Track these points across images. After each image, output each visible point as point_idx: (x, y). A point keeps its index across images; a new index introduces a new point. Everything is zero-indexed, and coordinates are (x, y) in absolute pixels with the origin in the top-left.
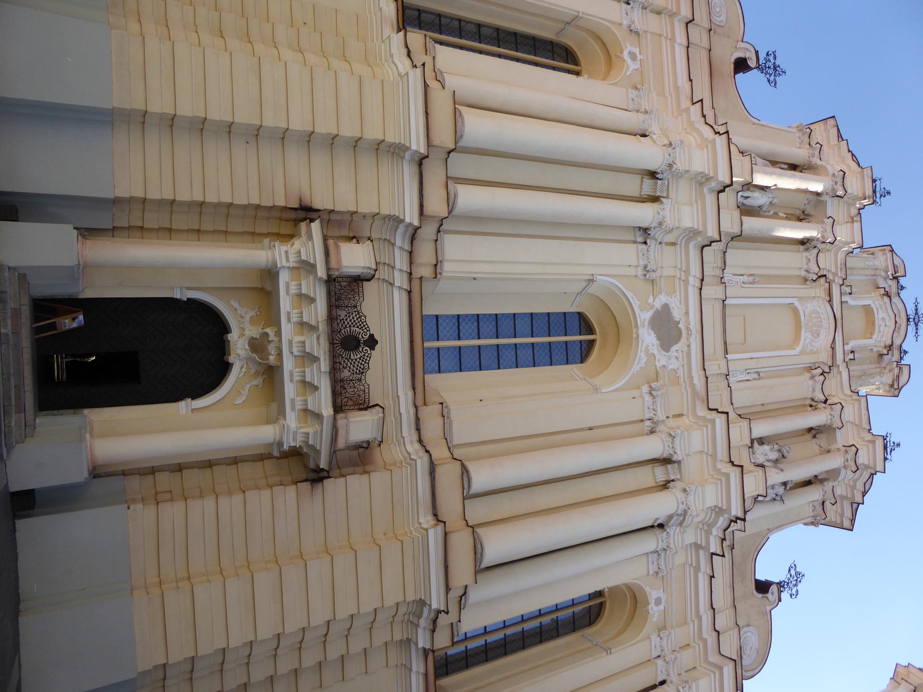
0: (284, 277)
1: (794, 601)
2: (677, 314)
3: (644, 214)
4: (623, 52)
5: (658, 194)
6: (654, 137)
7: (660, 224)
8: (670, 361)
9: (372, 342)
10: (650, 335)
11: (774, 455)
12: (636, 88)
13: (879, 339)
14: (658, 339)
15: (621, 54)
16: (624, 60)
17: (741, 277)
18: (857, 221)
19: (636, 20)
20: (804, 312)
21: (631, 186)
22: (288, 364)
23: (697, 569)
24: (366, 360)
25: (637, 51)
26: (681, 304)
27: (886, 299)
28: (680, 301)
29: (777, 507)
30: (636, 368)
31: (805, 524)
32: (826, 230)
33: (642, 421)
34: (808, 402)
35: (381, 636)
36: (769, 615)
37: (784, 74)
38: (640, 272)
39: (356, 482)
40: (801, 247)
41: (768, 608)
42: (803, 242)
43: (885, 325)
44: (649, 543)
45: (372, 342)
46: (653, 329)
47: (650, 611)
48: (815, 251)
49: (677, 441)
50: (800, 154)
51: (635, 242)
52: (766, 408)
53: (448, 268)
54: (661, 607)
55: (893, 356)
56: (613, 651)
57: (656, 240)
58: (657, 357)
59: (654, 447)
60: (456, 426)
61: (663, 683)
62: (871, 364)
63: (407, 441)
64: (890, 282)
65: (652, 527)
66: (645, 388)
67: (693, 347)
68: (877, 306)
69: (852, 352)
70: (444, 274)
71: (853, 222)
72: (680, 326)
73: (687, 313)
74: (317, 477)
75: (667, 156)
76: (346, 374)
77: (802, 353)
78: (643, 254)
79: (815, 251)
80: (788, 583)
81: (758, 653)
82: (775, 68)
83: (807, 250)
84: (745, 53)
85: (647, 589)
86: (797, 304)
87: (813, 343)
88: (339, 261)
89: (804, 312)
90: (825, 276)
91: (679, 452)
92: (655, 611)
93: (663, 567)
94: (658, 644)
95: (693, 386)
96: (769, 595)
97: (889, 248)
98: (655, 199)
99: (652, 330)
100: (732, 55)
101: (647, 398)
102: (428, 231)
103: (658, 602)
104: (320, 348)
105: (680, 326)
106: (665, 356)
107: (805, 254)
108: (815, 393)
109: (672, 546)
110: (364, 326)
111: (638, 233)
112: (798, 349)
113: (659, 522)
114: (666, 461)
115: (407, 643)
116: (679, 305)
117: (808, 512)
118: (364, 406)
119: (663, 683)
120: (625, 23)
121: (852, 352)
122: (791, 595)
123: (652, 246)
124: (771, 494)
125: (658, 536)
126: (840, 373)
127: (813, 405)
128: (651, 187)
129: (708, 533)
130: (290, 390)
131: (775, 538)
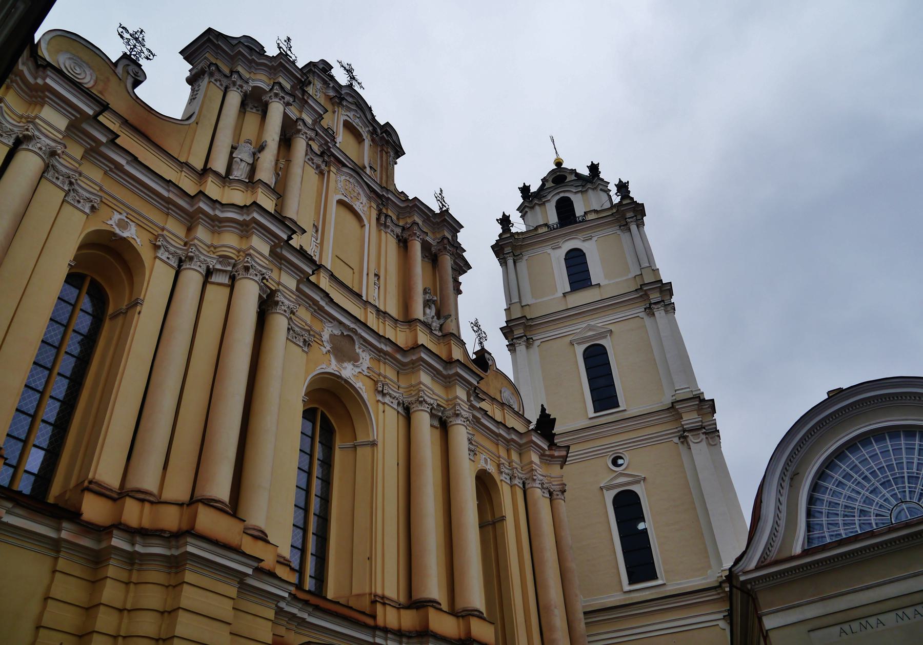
2: (337, 332)
4: (114, 234)
6: (218, 267)
10: (345, 368)
12: (158, 247)
13: (366, 134)
14: (350, 361)
15: (116, 237)
16: (124, 238)
18: (308, 98)
19: (88, 195)
20: (343, 194)
25: (117, 216)
26: (331, 322)
28: (330, 322)
32: (306, 133)
36: (498, 371)
37: (143, 33)
41: (495, 369)
43: (358, 118)
47: (490, 471)
56: (504, 515)
58: (361, 371)
66: (380, 398)
67: (364, 334)
68: (345, 114)
71: (307, 102)
72: (345, 334)
73: (340, 323)
75: (256, 278)
77: (370, 223)
78: (296, 338)
84: (128, 73)
89: (343, 194)
92: (491, 468)
95: (386, 353)
97: (311, 65)
99: (343, 363)
100: (129, 93)
101: (387, 400)
105: (345, 334)
106: (361, 363)
108: (395, 232)
112: (366, 222)
116: (331, 325)
120: (87, 211)
126: (388, 199)
128: (224, 276)
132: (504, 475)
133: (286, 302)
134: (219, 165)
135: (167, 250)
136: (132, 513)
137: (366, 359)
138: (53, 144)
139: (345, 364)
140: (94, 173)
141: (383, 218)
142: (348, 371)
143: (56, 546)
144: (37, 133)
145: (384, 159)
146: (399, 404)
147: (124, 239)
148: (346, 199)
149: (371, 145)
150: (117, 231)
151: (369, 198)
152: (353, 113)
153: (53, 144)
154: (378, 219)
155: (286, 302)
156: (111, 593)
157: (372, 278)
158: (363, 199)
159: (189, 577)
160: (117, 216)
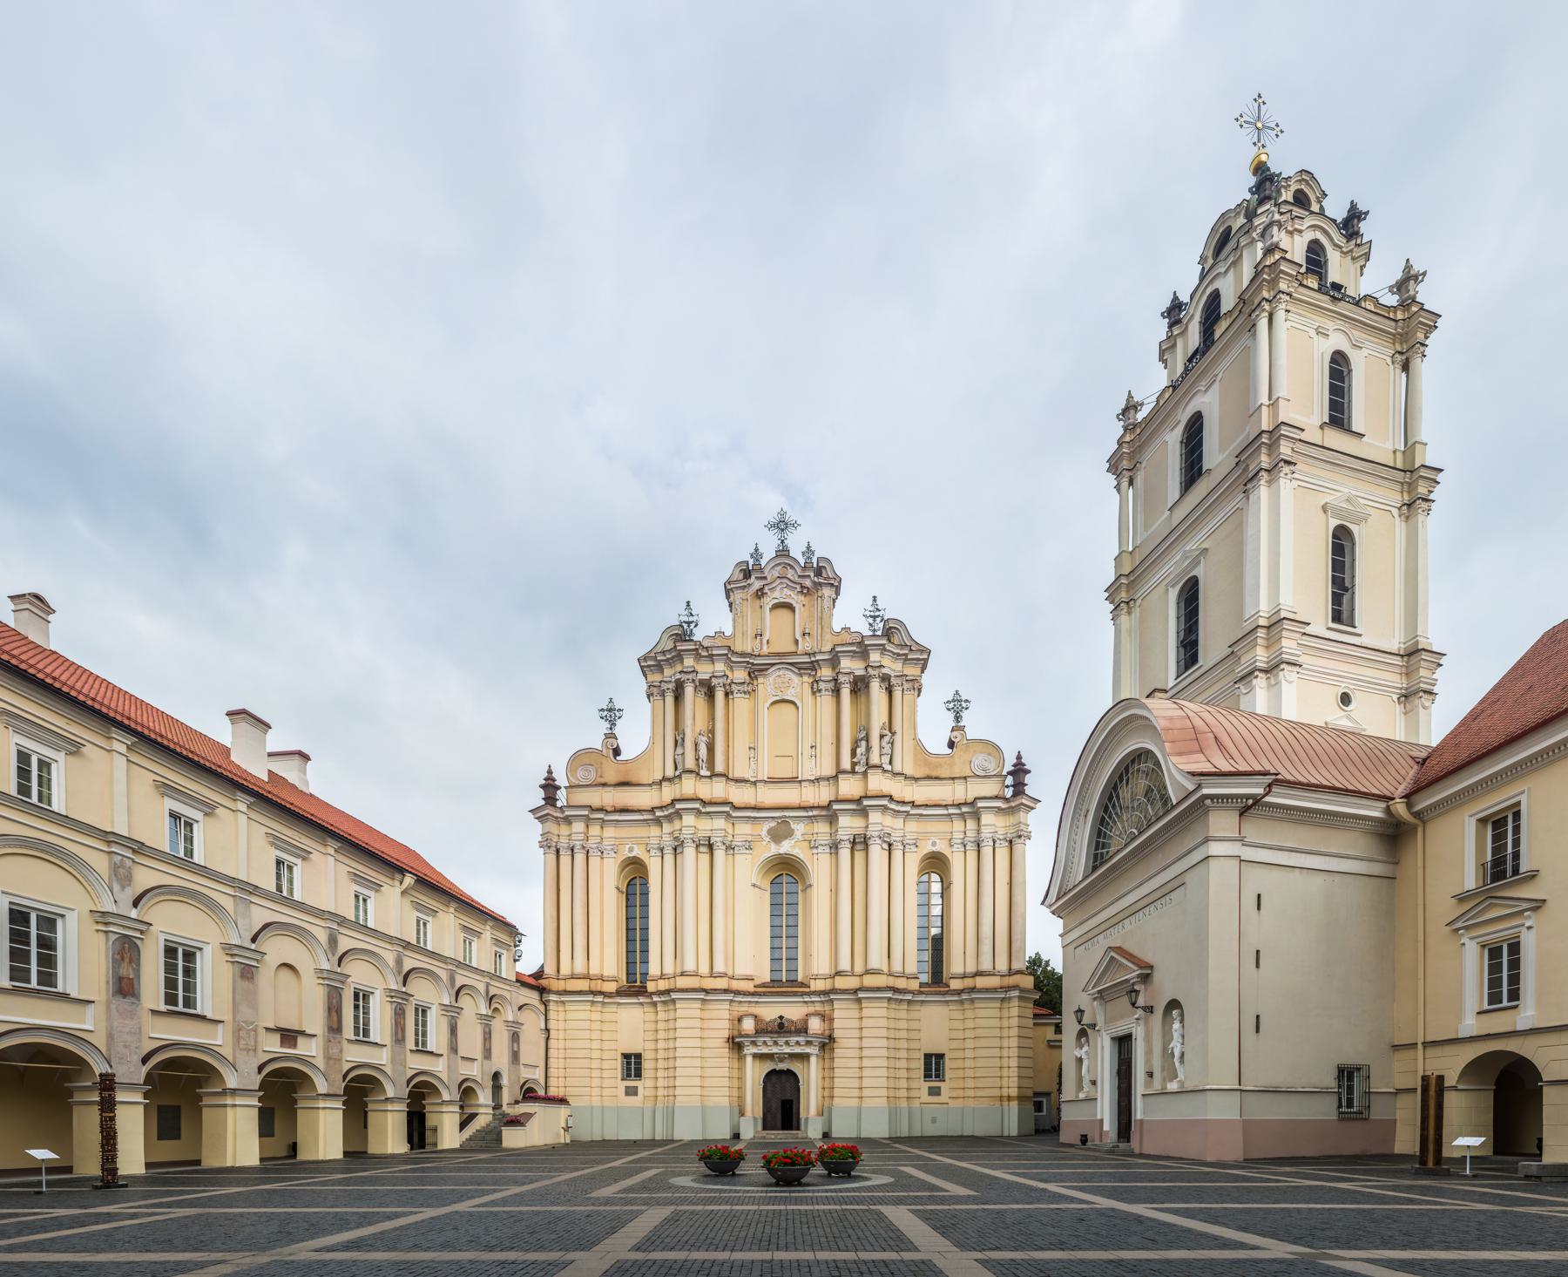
0: (755, 1050)
1: (971, 705)
2: (773, 824)
3: (720, 854)
5: (707, 843)
7: (724, 844)
8: (799, 829)
9: (781, 1017)
11: (863, 743)
13: (795, 597)
14: (786, 838)
17: (752, 759)
21: (704, 859)
22: (787, 1050)
23: (921, 815)
24: (788, 1020)
25: (627, 846)
27: (766, 590)
29: (898, 738)
30: (801, 856)
31: (919, 695)
33: (831, 854)
34: (835, 694)
35: (903, 1014)
38: (751, 852)
39: (836, 1024)
40: (731, 697)
41: (965, 742)
42: (727, 694)
44: (897, 855)
45: (781, 1017)
46: (780, 842)
48: (733, 685)
49: (843, 838)
50: (670, 699)
51: (733, 855)
52: (835, 742)
53: (749, 972)
54: (938, 841)
55: (809, 576)
57: (732, 841)
59: (845, 853)
60: (821, 972)
61: (978, 845)
62: (813, 606)
63: (823, 999)
64: (753, 577)
65: (890, 849)
66: (815, 851)
69: (804, 635)
70: (752, 973)
74: (831, 1038)
76: (793, 1028)
79: (733, 685)
80: (958, 713)
81: (989, 754)
82: (610, 710)
83: (732, 693)
85: (925, 852)
86: (767, 704)
87: (795, 685)
88: (749, 1030)
90: (749, 673)
91: (847, 837)
92: (941, 847)
93: (914, 841)
94: (959, 846)
95: (814, 816)
96: (956, 740)
97: (727, 584)
98: (711, 847)
101: (820, 849)
102: (736, 985)
103: (934, 844)
104: (781, 1040)
107: (735, 695)
109: (901, 839)
110: (775, 1020)
111: (728, 852)
112: (799, 704)
113: (887, 848)
114: (854, 843)
115: (909, 1002)
117: (909, 696)
118: (806, 1022)
119: (978, 845)
120: (614, 855)
121: (804, 635)
122: (967, 709)
123: (737, 843)
124: (887, 749)
125: (895, 847)
126: (817, 661)
127: (837, 692)
129: (899, 812)
130: (798, 1050)
131: (920, 736)
132: (956, 846)
133: (718, 839)
134: (670, 772)
135: (654, 849)
136: (663, 985)
137: (799, 829)
138: (581, 842)
139: (783, 843)
140: (609, 832)
141: (815, 685)
142: (786, 847)
143: (641, 1004)
144: (575, 842)
145: (819, 605)
146: (831, 848)
147: (634, 857)
148: (778, 698)
149: (804, 605)
150: (630, 855)
151: (801, 675)
152: (778, 589)
153: (581, 842)
154: (812, 688)
155: (718, 839)
156: (661, 1015)
157: (808, 751)
158: (796, 679)
159: (678, 1006)
160: (627, 846)
